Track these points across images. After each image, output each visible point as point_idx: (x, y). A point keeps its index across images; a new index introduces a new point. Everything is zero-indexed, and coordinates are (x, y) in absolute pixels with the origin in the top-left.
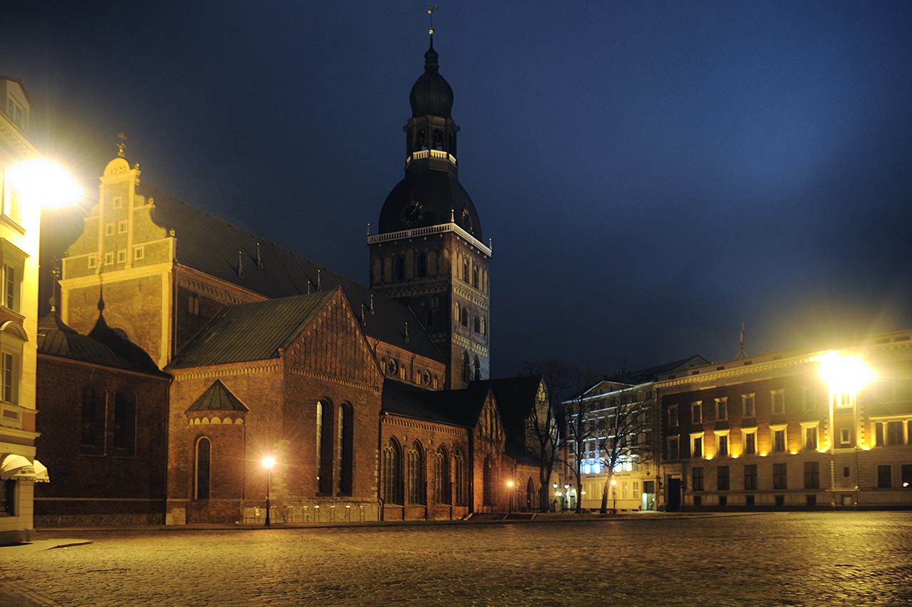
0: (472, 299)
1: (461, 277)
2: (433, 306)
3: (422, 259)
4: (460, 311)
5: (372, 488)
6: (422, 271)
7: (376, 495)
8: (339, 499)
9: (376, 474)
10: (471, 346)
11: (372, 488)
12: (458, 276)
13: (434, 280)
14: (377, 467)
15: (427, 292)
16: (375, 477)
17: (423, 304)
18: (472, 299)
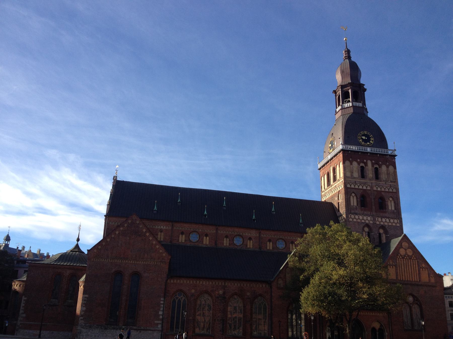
0: (372, 187)
1: (356, 175)
3: (334, 170)
4: (357, 198)
5: (156, 322)
7: (160, 326)
9: (161, 313)
10: (374, 220)
11: (156, 322)
12: (352, 175)
13: (339, 182)
14: (162, 309)
15: (337, 191)
16: (160, 315)
17: (336, 199)
18: (372, 187)
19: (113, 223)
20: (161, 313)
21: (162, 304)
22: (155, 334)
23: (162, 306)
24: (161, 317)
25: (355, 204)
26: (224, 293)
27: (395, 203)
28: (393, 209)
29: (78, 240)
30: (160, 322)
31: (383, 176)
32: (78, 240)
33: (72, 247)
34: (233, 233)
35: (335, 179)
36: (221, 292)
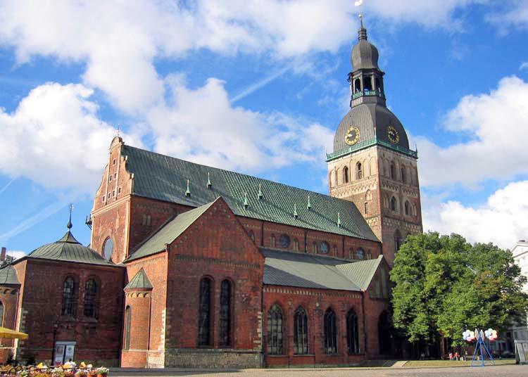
2: (368, 199)
5: (256, 342)
6: (359, 176)
8: (221, 350)
9: (259, 330)
11: (256, 342)
14: (260, 325)
19: (141, 207)
20: (259, 330)
21: (260, 319)
22: (256, 357)
23: (260, 321)
24: (260, 336)
25: (387, 207)
26: (321, 305)
27: (417, 208)
28: (416, 215)
29: (70, 226)
30: (259, 342)
31: (408, 180)
32: (70, 226)
33: (61, 234)
34: (279, 232)
35: (359, 176)
36: (318, 305)
